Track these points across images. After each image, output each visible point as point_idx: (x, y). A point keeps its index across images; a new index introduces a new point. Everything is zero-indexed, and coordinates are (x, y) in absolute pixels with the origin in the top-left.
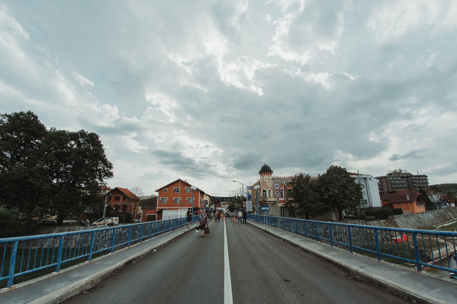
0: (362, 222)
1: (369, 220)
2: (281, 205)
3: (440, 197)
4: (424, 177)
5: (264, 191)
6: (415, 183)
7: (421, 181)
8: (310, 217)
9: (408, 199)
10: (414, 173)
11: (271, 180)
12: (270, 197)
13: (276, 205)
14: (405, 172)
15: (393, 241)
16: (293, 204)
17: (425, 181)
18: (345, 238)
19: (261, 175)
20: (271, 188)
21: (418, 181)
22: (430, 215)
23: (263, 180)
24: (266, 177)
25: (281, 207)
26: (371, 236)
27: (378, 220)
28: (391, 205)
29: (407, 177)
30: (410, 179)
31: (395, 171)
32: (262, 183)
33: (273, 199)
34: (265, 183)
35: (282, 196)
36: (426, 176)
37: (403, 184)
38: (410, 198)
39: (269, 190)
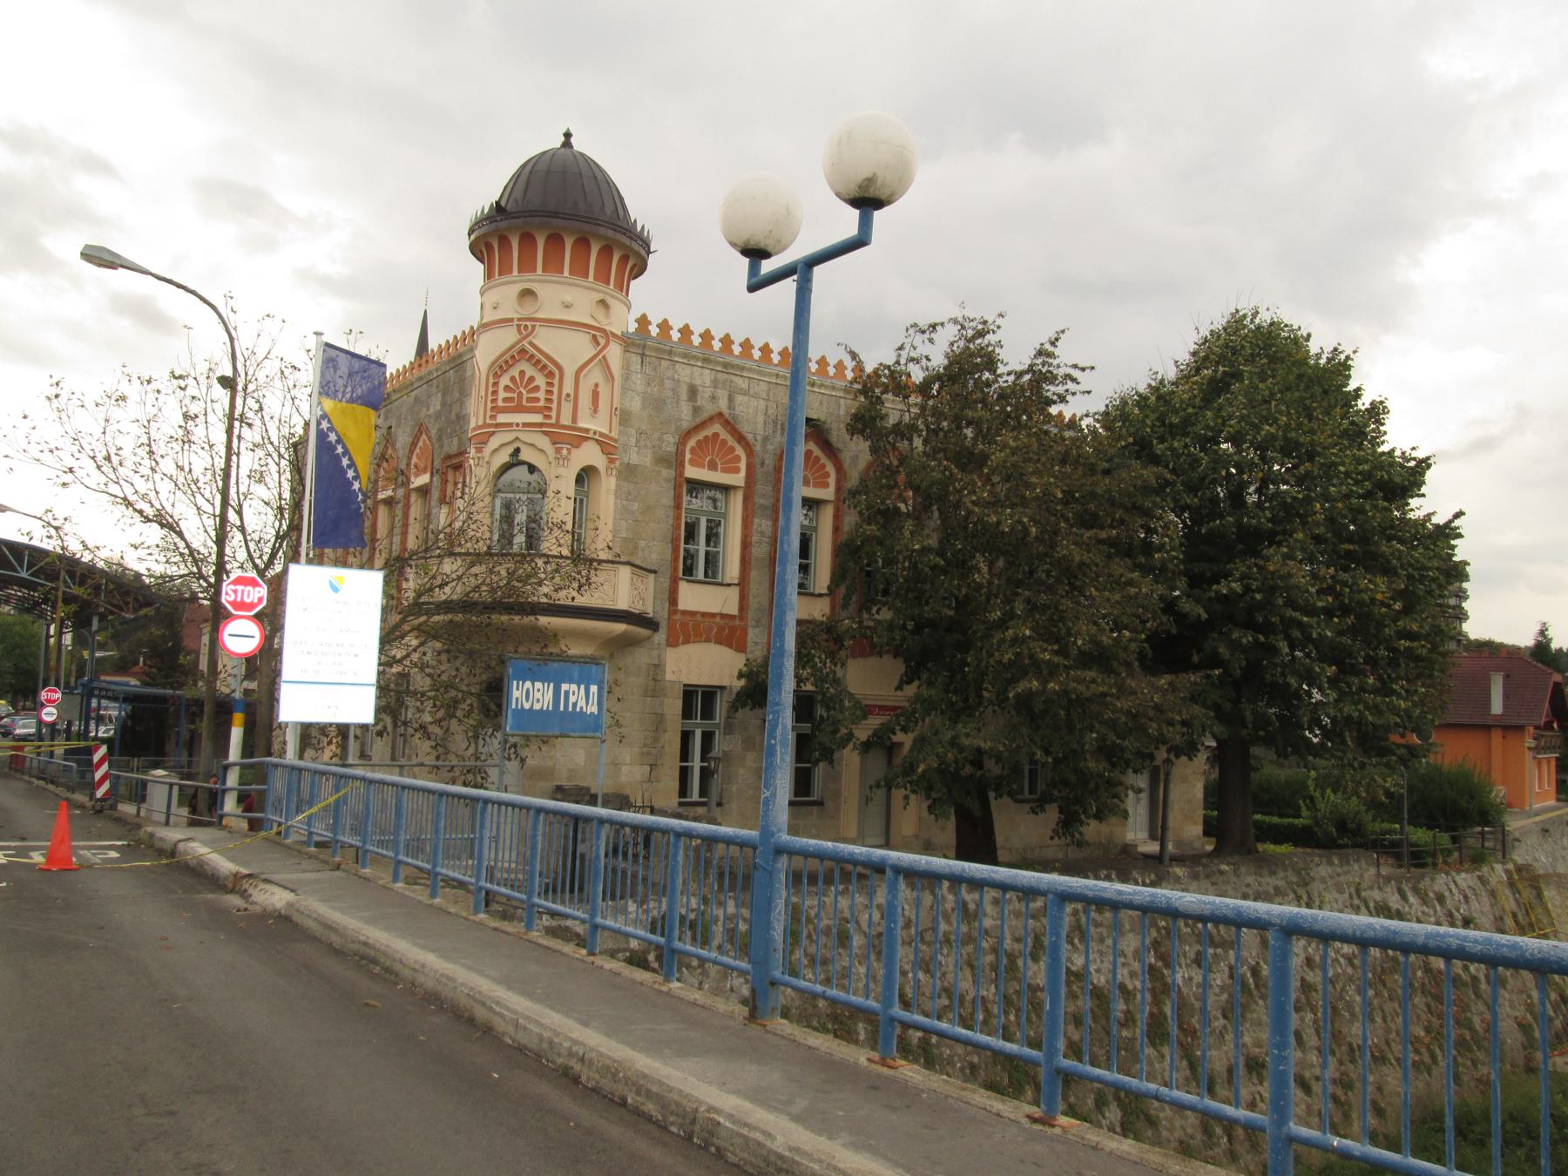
1: (1419, 859)
8: (1014, 824)
9: (1497, 707)
11: (614, 353)
13: (641, 658)
18: (1312, 1040)
20: (606, 445)
23: (526, 326)
24: (566, 296)
25: (689, 693)
26: (1465, 1008)
27: (1478, 860)
32: (501, 366)
33: (620, 590)
34: (550, 368)
38: (1506, 697)
39: (586, 476)
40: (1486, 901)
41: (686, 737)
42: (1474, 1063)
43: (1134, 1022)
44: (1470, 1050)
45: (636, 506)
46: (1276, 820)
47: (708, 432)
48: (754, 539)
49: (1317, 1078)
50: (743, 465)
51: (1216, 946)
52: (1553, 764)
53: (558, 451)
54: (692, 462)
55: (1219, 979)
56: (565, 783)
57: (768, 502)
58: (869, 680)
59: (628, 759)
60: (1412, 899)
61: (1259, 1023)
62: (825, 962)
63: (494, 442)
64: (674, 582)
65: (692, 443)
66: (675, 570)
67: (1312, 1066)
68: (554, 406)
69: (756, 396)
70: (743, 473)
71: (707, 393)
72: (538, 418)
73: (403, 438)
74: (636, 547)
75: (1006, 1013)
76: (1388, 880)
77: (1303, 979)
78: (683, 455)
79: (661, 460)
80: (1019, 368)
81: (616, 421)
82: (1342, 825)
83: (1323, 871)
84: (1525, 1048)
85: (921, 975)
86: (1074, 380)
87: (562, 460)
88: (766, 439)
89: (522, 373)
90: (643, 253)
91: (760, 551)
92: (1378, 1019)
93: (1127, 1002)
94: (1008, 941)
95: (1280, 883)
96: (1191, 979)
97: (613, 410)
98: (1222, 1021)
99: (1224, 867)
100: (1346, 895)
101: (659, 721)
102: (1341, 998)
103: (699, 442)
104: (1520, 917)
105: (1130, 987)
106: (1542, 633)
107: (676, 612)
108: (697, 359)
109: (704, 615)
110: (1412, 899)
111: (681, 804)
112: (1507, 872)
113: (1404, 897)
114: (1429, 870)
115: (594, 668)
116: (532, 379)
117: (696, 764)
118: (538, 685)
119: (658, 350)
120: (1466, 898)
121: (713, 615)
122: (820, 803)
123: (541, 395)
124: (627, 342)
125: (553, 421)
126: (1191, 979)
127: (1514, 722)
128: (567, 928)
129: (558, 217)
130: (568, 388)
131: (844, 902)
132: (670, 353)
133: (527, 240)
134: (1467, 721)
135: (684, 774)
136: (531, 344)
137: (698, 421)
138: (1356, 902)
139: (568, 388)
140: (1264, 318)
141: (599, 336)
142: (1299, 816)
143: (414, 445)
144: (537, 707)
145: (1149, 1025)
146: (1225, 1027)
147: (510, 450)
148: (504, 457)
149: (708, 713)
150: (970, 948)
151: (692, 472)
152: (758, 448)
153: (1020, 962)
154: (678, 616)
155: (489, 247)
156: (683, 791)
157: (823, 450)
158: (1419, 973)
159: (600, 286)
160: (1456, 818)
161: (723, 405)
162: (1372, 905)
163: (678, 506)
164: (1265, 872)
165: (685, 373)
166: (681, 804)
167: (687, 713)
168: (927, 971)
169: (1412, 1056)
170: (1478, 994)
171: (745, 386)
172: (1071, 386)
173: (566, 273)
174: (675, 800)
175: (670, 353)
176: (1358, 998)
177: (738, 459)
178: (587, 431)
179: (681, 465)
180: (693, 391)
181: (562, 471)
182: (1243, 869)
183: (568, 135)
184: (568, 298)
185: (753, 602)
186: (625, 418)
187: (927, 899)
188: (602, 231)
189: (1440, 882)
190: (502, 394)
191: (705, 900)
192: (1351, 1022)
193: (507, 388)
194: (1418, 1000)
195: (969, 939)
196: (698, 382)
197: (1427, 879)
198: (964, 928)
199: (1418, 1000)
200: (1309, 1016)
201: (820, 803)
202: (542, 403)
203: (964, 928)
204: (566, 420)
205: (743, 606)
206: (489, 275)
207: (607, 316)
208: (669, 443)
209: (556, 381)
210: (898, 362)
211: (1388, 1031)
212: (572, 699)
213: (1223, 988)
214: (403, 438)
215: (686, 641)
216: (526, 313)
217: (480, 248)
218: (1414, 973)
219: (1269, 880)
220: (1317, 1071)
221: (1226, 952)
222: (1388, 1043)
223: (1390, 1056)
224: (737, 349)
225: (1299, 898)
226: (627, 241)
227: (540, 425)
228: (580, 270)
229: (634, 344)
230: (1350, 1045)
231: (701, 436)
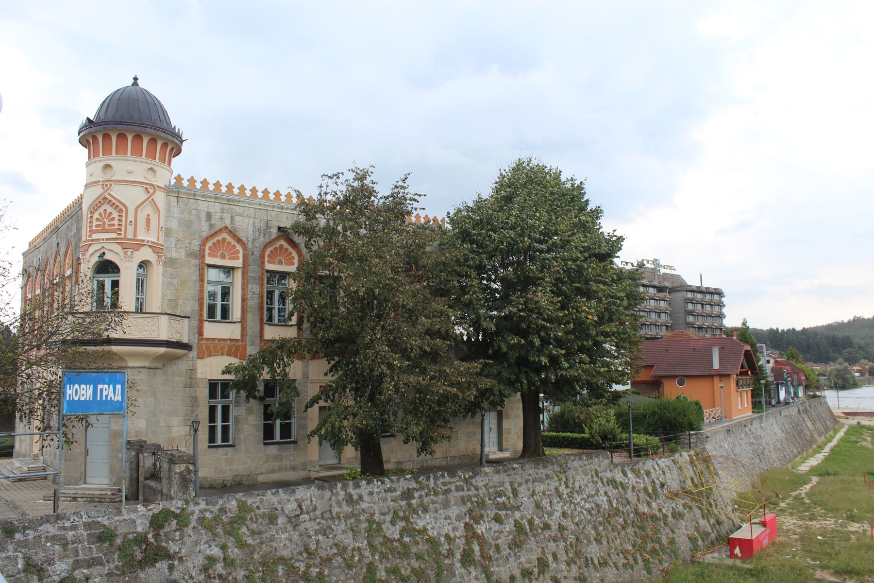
0: (623, 465)
1: (639, 452)
2: (213, 368)
3: (772, 361)
4: (716, 297)
5: (106, 267)
6: (691, 313)
7: (708, 308)
9: (716, 365)
10: (693, 281)
11: (160, 198)
12: (140, 310)
13: (182, 366)
14: (668, 271)
15: (737, 551)
16: (295, 369)
17: (717, 308)
18: (562, 557)
19: (93, 155)
21: (699, 306)
22: (772, 428)
24: (130, 166)
25: (213, 385)
26: (657, 531)
27: (673, 451)
28: (656, 384)
29: (672, 290)
30: (679, 296)
31: (641, 265)
32: (94, 208)
33: (163, 329)
34: (120, 207)
35: (225, 313)
36: (719, 293)
37: (659, 314)
38: (721, 359)
40: (675, 472)
41: (212, 409)
42: (660, 562)
43: (453, 555)
44: (658, 555)
45: (176, 281)
46: (575, 435)
47: (220, 238)
48: (249, 296)
49: (565, 578)
50: (241, 255)
51: (507, 510)
52: (750, 393)
53: (126, 253)
54: (210, 255)
55: (509, 526)
56: (133, 438)
57: (257, 275)
58: (310, 374)
59: (176, 423)
60: (630, 475)
61: (531, 550)
62: (260, 533)
63: (92, 250)
64: (201, 322)
65: (209, 244)
66: (201, 315)
67: (562, 571)
68: (123, 228)
69: (248, 216)
70: (241, 260)
71: (218, 216)
72: (114, 235)
73: (63, 249)
74: (177, 304)
75: (373, 555)
76: (616, 466)
77: (559, 524)
78: (204, 251)
79: (191, 255)
80: (386, 195)
81: (162, 234)
82: (605, 438)
83: (576, 464)
84: (692, 551)
85: (320, 537)
86: (415, 200)
87: (128, 258)
88: (254, 240)
89: (105, 210)
90: (176, 141)
91: (253, 302)
92: (604, 543)
93: (449, 544)
94: (377, 515)
95: (549, 472)
96: (490, 529)
97: (160, 229)
98: (508, 551)
99: (516, 466)
100: (590, 476)
101: (194, 401)
102: (583, 532)
103: (214, 244)
104: (695, 480)
105: (452, 536)
106: (744, 324)
107: (202, 339)
108: (211, 197)
109: (220, 340)
110: (630, 475)
111: (210, 447)
112: (689, 456)
113: (625, 474)
114: (643, 458)
115: (118, 375)
116: (111, 213)
117: (219, 424)
118: (83, 386)
119: (187, 194)
120: (664, 472)
121: (225, 340)
122: (295, 442)
123: (116, 222)
124: (168, 190)
125: (122, 236)
126: (490, 529)
127: (725, 373)
128: (98, 522)
129: (129, 124)
130: (131, 217)
131: (275, 499)
132: (195, 195)
133: (107, 137)
134: (701, 373)
135: (212, 430)
136: (109, 194)
137: (213, 232)
138: (596, 479)
139: (131, 217)
140: (534, 163)
141: (149, 188)
142: (583, 432)
143: (67, 252)
144: (83, 398)
145: (463, 556)
146: (509, 554)
147: (99, 254)
148: (95, 259)
149: (225, 396)
150: (353, 520)
151: (209, 260)
152: (250, 245)
153: (383, 526)
154: (204, 342)
155: (88, 141)
156: (212, 439)
157: (289, 244)
158: (632, 515)
159: (150, 161)
160: (673, 428)
161: (227, 222)
162: (605, 480)
163: (202, 279)
164: (541, 466)
165: (203, 206)
166: (210, 447)
167: (212, 395)
168: (325, 534)
169: (624, 561)
170: (666, 524)
171: (241, 211)
172: (415, 205)
173: (129, 155)
174: (207, 444)
175: (195, 195)
176: (593, 532)
177: (238, 252)
178: (143, 241)
179: (203, 257)
180: (209, 216)
181: (128, 264)
182: (527, 466)
183: (136, 79)
184: (130, 168)
185: (249, 332)
186: (168, 233)
187: (328, 494)
188: (148, 130)
189: (649, 464)
190: (95, 223)
191: (187, 502)
192: (588, 545)
193: (97, 219)
194: (630, 530)
195: (353, 515)
196: (212, 210)
197: (641, 464)
198: (350, 510)
199: (630, 530)
200: (562, 544)
201: (295, 442)
202: (116, 227)
203: (350, 510)
204: (130, 235)
205: (243, 334)
206: (89, 158)
207: (155, 177)
208: (195, 245)
209: (124, 214)
210: (320, 194)
211: (610, 548)
212: (105, 393)
213: (510, 533)
214: (63, 249)
215: (210, 355)
216: (107, 178)
217: (84, 142)
218: (628, 515)
219: (543, 471)
220: (565, 574)
221: (513, 512)
222: (609, 555)
223: (610, 562)
224: (236, 191)
225: (560, 480)
226: (164, 135)
227: (116, 239)
228: (137, 152)
229: (172, 191)
230: (586, 558)
231: (215, 240)
